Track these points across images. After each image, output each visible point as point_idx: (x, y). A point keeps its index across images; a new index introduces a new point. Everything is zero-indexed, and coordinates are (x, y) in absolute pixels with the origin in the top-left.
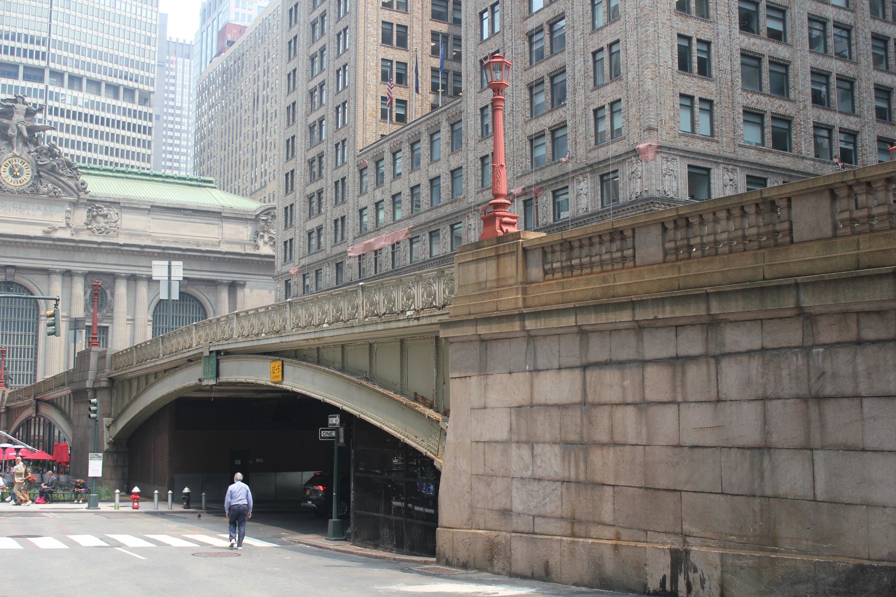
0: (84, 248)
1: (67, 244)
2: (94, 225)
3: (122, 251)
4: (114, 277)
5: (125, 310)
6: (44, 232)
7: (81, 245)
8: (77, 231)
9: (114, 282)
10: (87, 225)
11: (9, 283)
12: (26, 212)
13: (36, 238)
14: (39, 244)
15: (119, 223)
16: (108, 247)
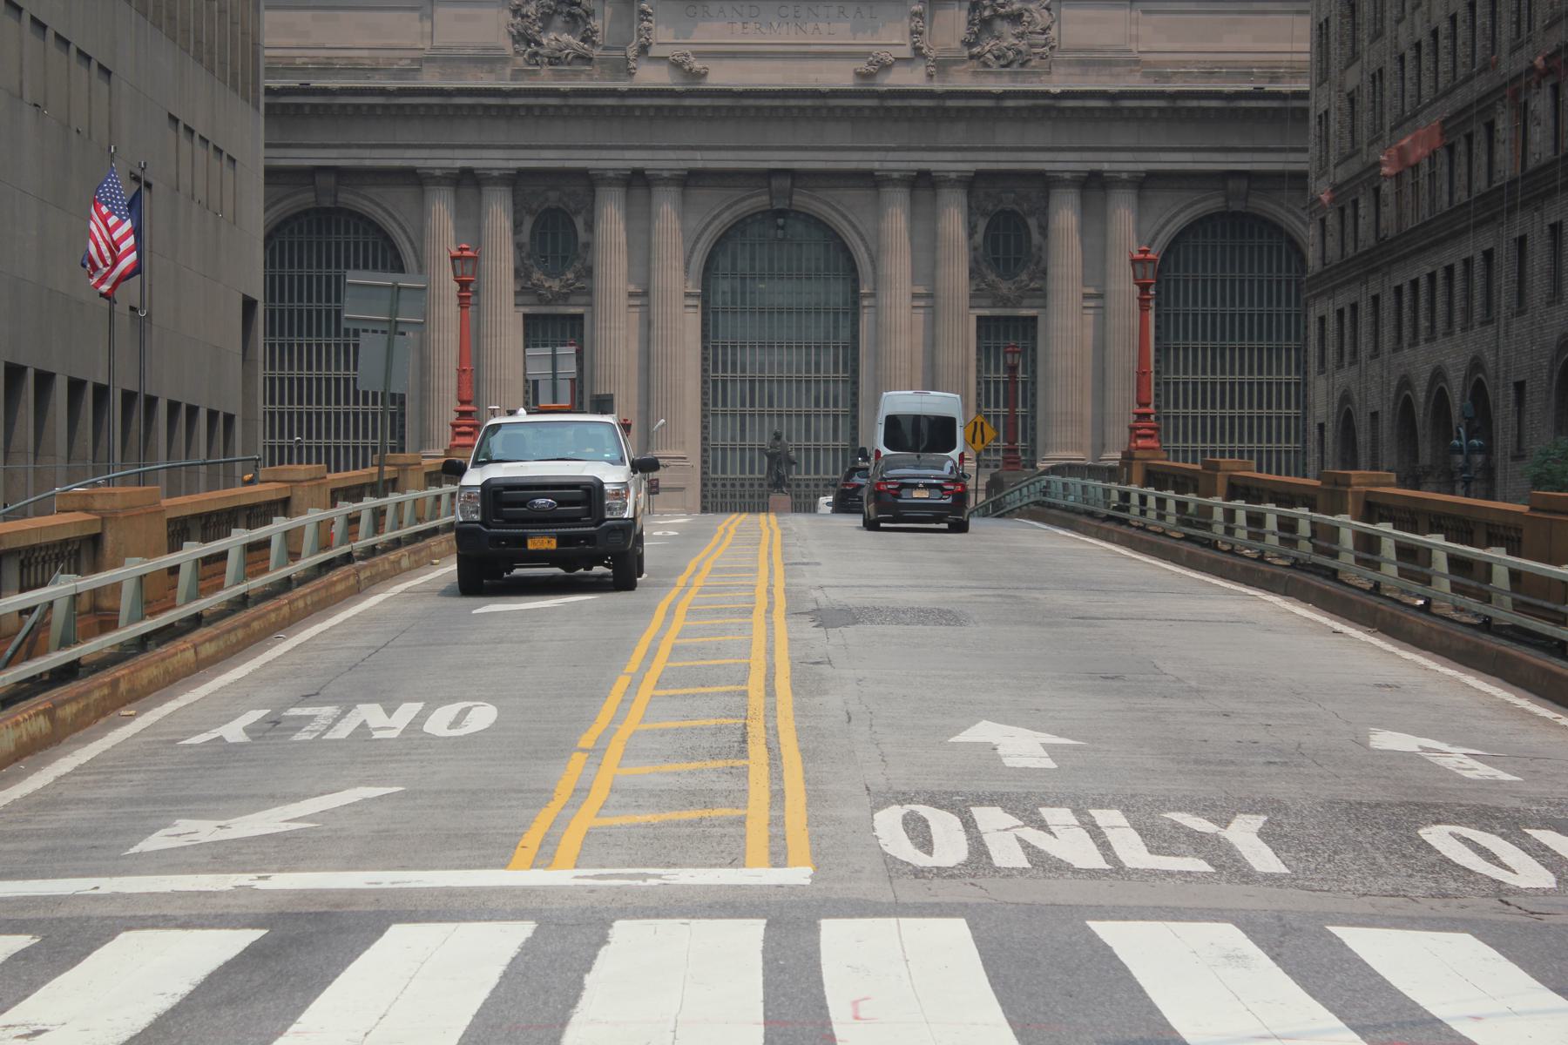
0: (959, 110)
1: (916, 103)
2: (988, 45)
3: (1062, 110)
4: (1045, 182)
5: (1077, 271)
6: (859, 74)
7: (950, 103)
8: (942, 66)
9: (1047, 198)
10: (969, 45)
11: (781, 213)
12: (810, 26)
13: (835, 94)
14: (845, 109)
15: (1053, 33)
16: (1022, 103)
